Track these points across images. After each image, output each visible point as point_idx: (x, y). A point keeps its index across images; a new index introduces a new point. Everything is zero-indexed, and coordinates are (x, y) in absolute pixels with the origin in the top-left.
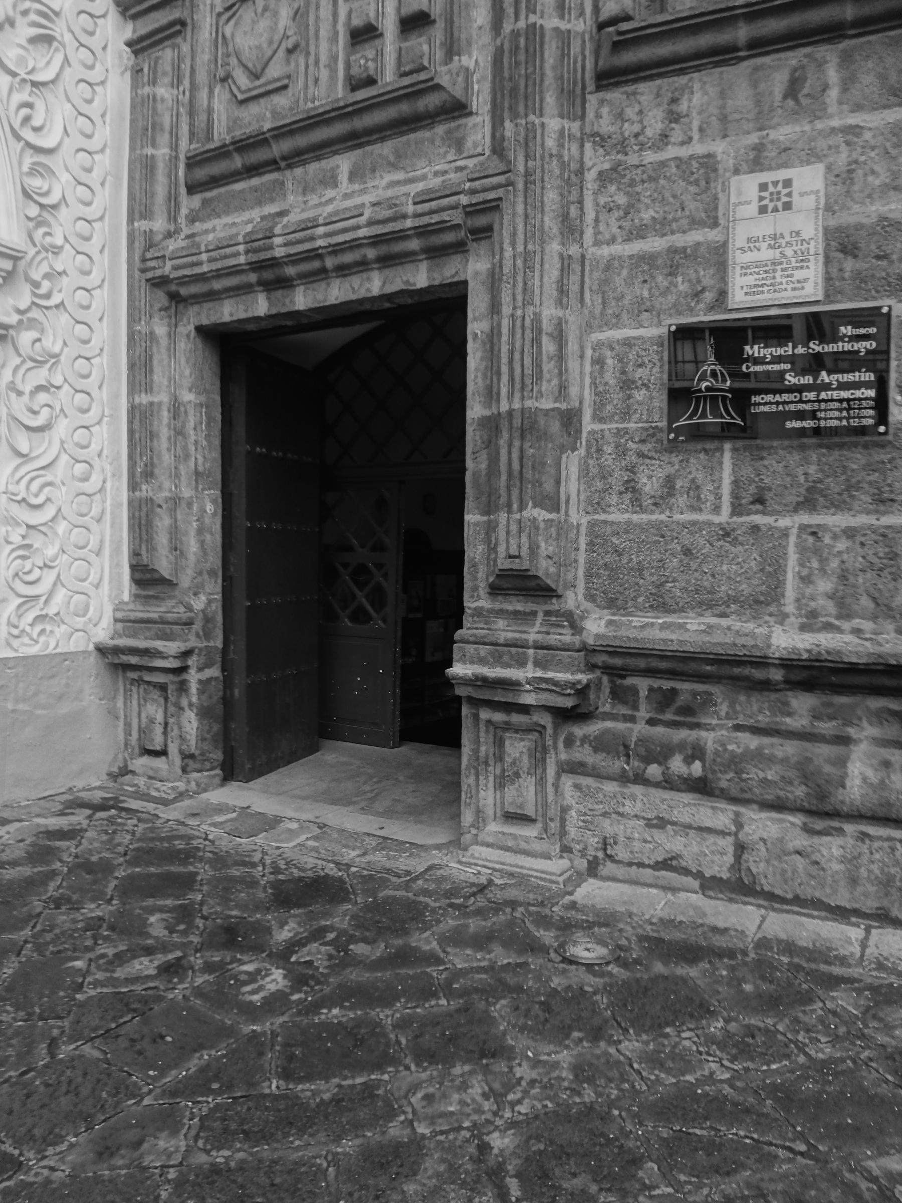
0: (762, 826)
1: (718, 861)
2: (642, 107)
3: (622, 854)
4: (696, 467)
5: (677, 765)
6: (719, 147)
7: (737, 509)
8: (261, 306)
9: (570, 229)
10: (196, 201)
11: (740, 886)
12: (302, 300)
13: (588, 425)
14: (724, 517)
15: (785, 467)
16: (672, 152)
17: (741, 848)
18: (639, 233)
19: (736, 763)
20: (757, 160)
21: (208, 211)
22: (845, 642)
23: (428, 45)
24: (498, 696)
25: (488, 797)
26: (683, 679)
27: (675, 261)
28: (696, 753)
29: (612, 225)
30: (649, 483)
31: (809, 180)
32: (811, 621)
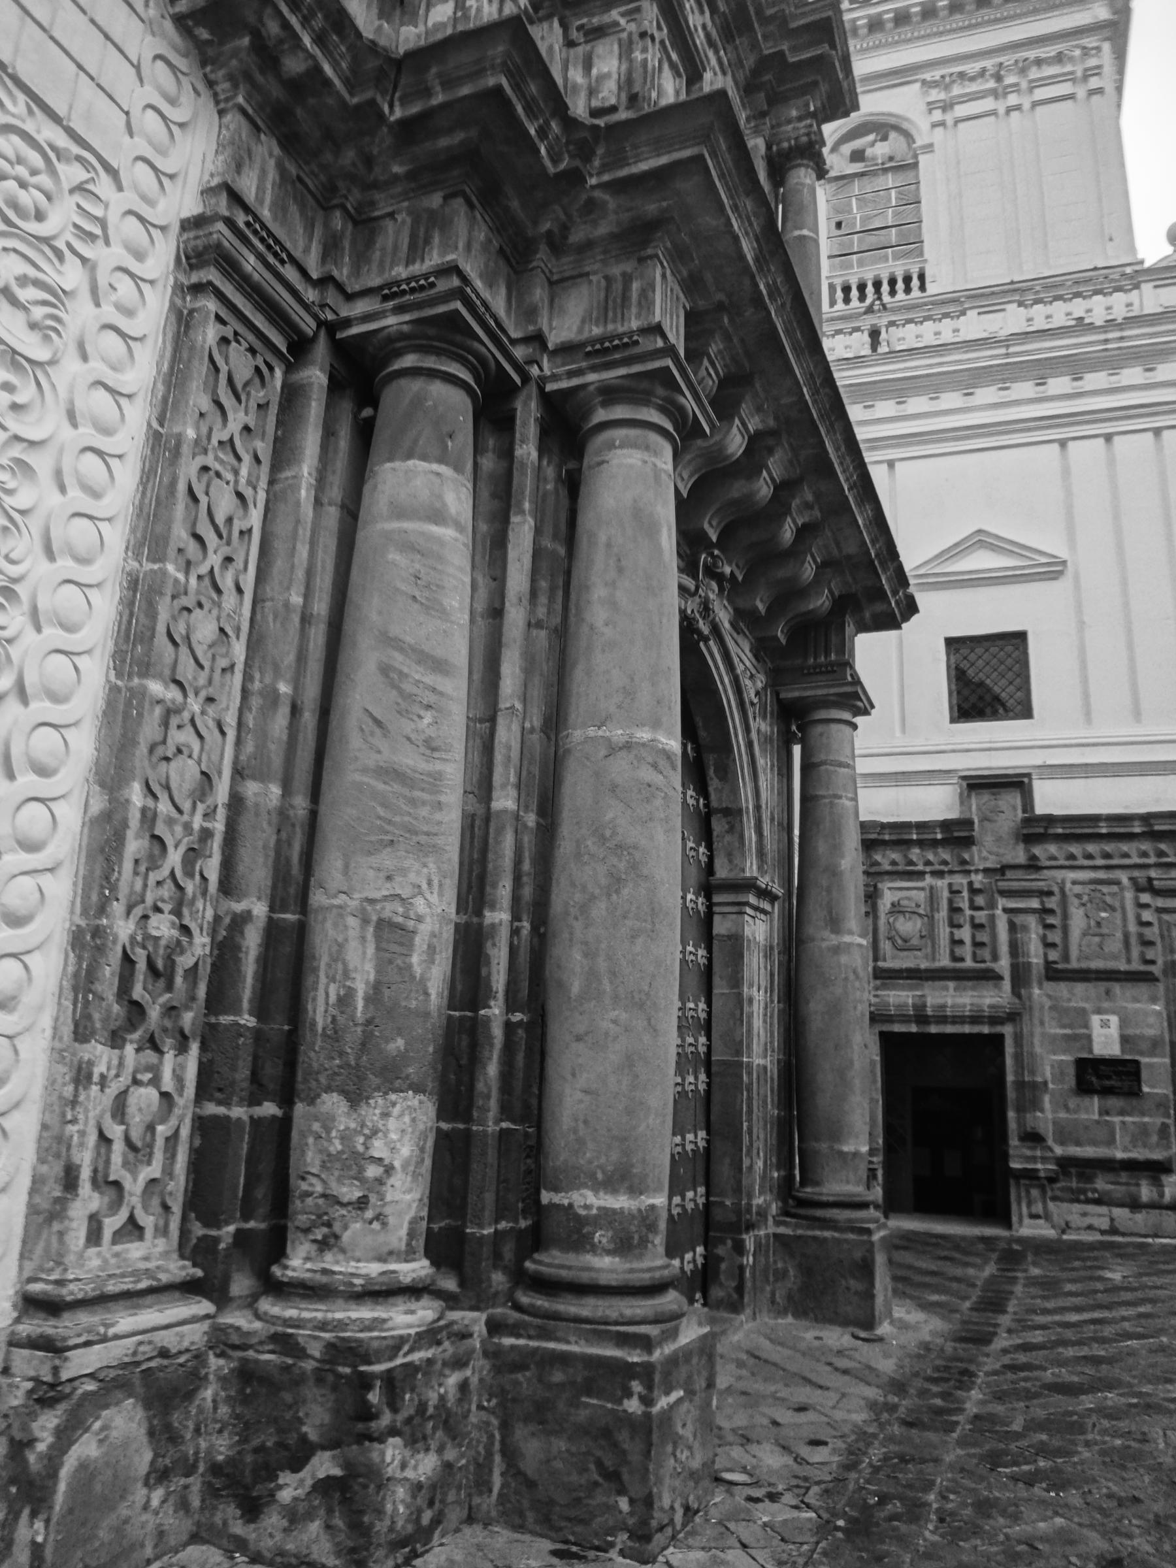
0: (1118, 1212)
1: (1104, 1224)
2: (1062, 989)
3: (1073, 1225)
4: (1086, 1101)
5: (1090, 1195)
6: (1086, 1005)
7: (1100, 1114)
8: (914, 1028)
9: (1042, 1023)
10: (878, 982)
11: (1113, 1231)
12: (933, 1029)
13: (1051, 1086)
14: (1096, 1117)
15: (1114, 1102)
16: (1073, 1004)
17: (1112, 1220)
18: (1064, 1026)
19: (1108, 1192)
20: (1099, 1011)
21: (884, 987)
22: (1139, 1154)
23: (986, 953)
24: (1030, 1175)
25: (1025, 1210)
26: (1087, 1168)
27: (1074, 1038)
28: (1095, 1190)
29: (1054, 1023)
30: (1071, 1105)
31: (1114, 1020)
32: (1125, 1149)
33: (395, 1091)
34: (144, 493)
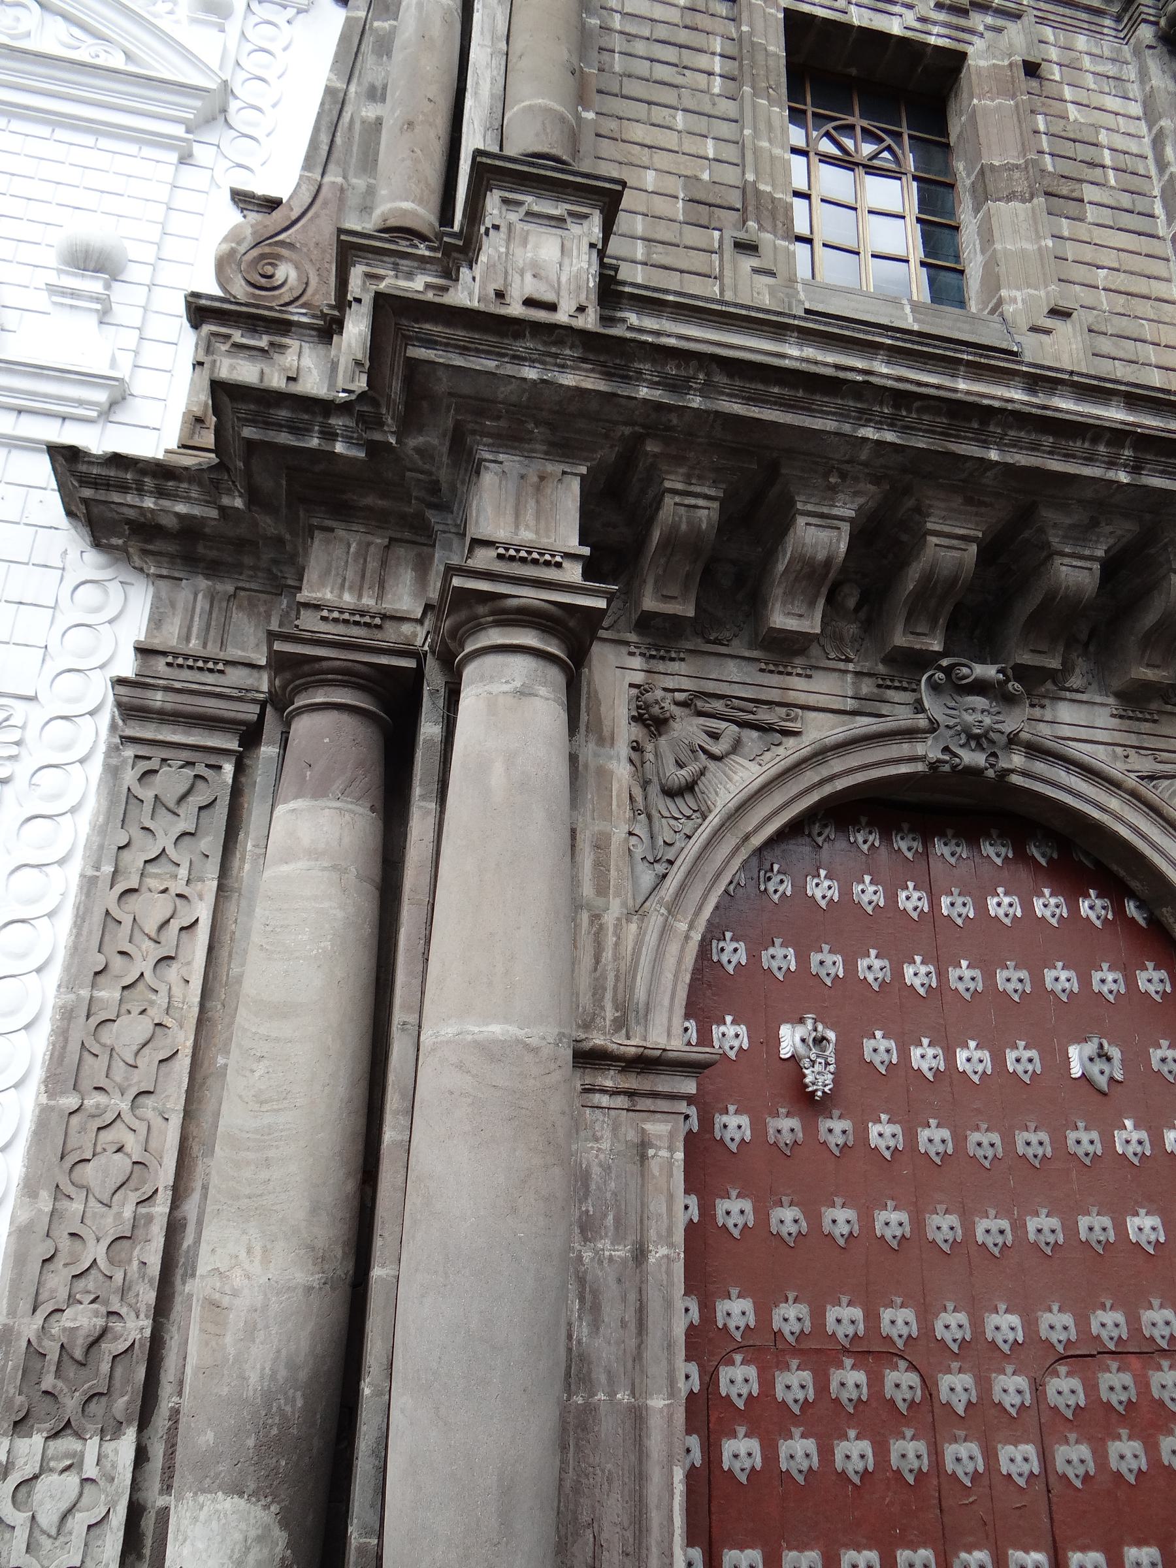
33: (203, 1491)
34: (78, 935)
